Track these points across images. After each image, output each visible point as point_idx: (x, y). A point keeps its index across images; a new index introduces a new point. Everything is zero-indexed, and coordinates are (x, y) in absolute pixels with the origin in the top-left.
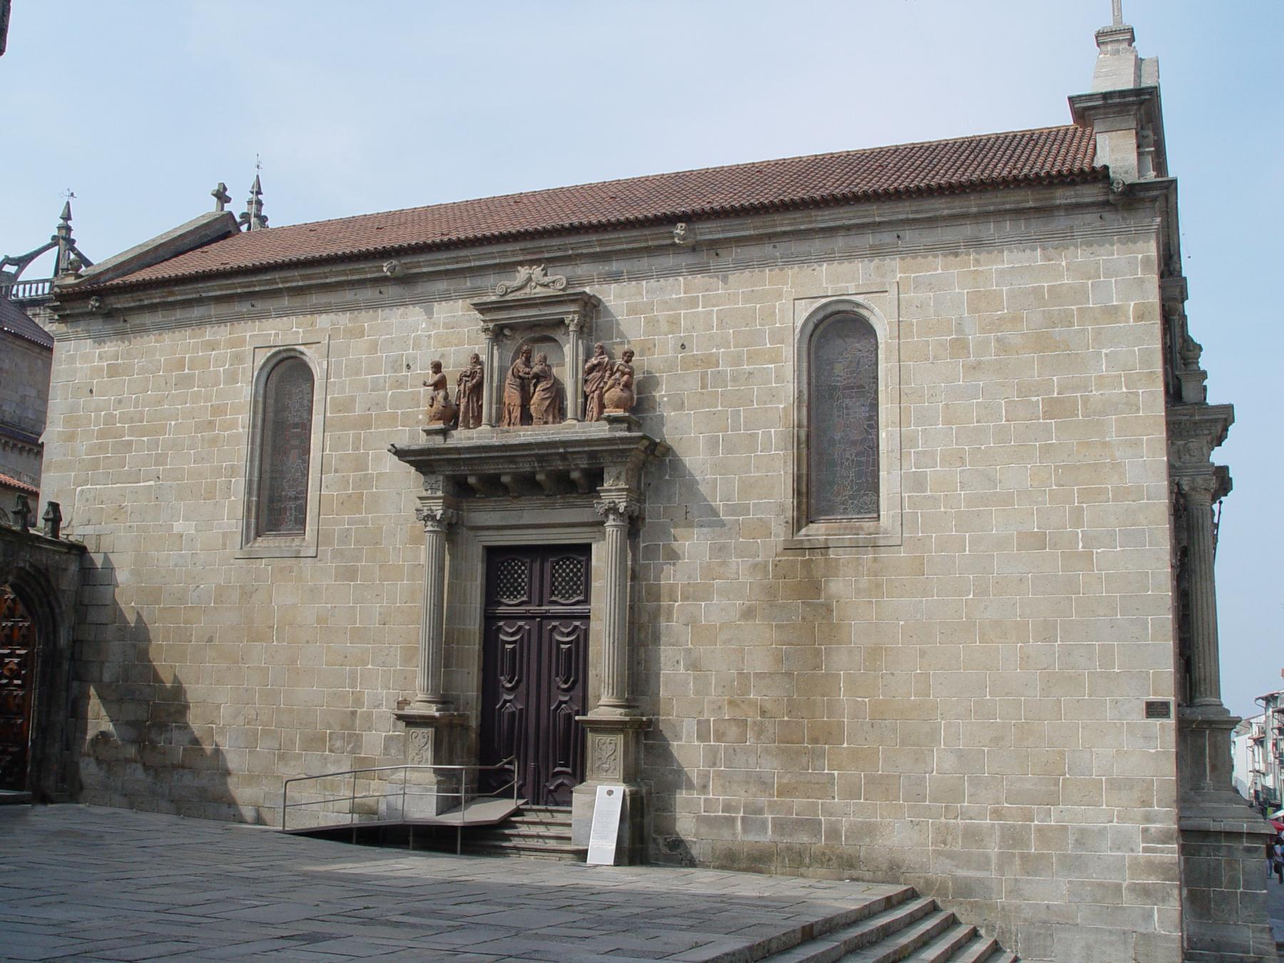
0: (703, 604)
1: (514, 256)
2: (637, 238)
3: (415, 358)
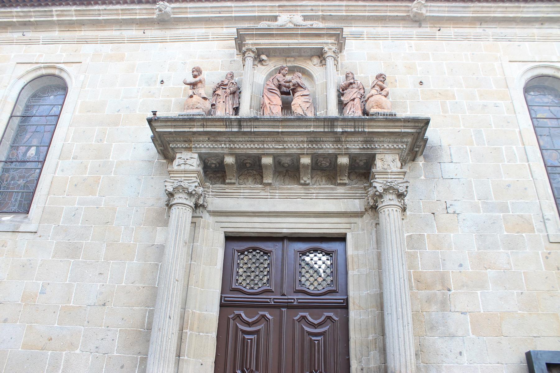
0: (479, 292)
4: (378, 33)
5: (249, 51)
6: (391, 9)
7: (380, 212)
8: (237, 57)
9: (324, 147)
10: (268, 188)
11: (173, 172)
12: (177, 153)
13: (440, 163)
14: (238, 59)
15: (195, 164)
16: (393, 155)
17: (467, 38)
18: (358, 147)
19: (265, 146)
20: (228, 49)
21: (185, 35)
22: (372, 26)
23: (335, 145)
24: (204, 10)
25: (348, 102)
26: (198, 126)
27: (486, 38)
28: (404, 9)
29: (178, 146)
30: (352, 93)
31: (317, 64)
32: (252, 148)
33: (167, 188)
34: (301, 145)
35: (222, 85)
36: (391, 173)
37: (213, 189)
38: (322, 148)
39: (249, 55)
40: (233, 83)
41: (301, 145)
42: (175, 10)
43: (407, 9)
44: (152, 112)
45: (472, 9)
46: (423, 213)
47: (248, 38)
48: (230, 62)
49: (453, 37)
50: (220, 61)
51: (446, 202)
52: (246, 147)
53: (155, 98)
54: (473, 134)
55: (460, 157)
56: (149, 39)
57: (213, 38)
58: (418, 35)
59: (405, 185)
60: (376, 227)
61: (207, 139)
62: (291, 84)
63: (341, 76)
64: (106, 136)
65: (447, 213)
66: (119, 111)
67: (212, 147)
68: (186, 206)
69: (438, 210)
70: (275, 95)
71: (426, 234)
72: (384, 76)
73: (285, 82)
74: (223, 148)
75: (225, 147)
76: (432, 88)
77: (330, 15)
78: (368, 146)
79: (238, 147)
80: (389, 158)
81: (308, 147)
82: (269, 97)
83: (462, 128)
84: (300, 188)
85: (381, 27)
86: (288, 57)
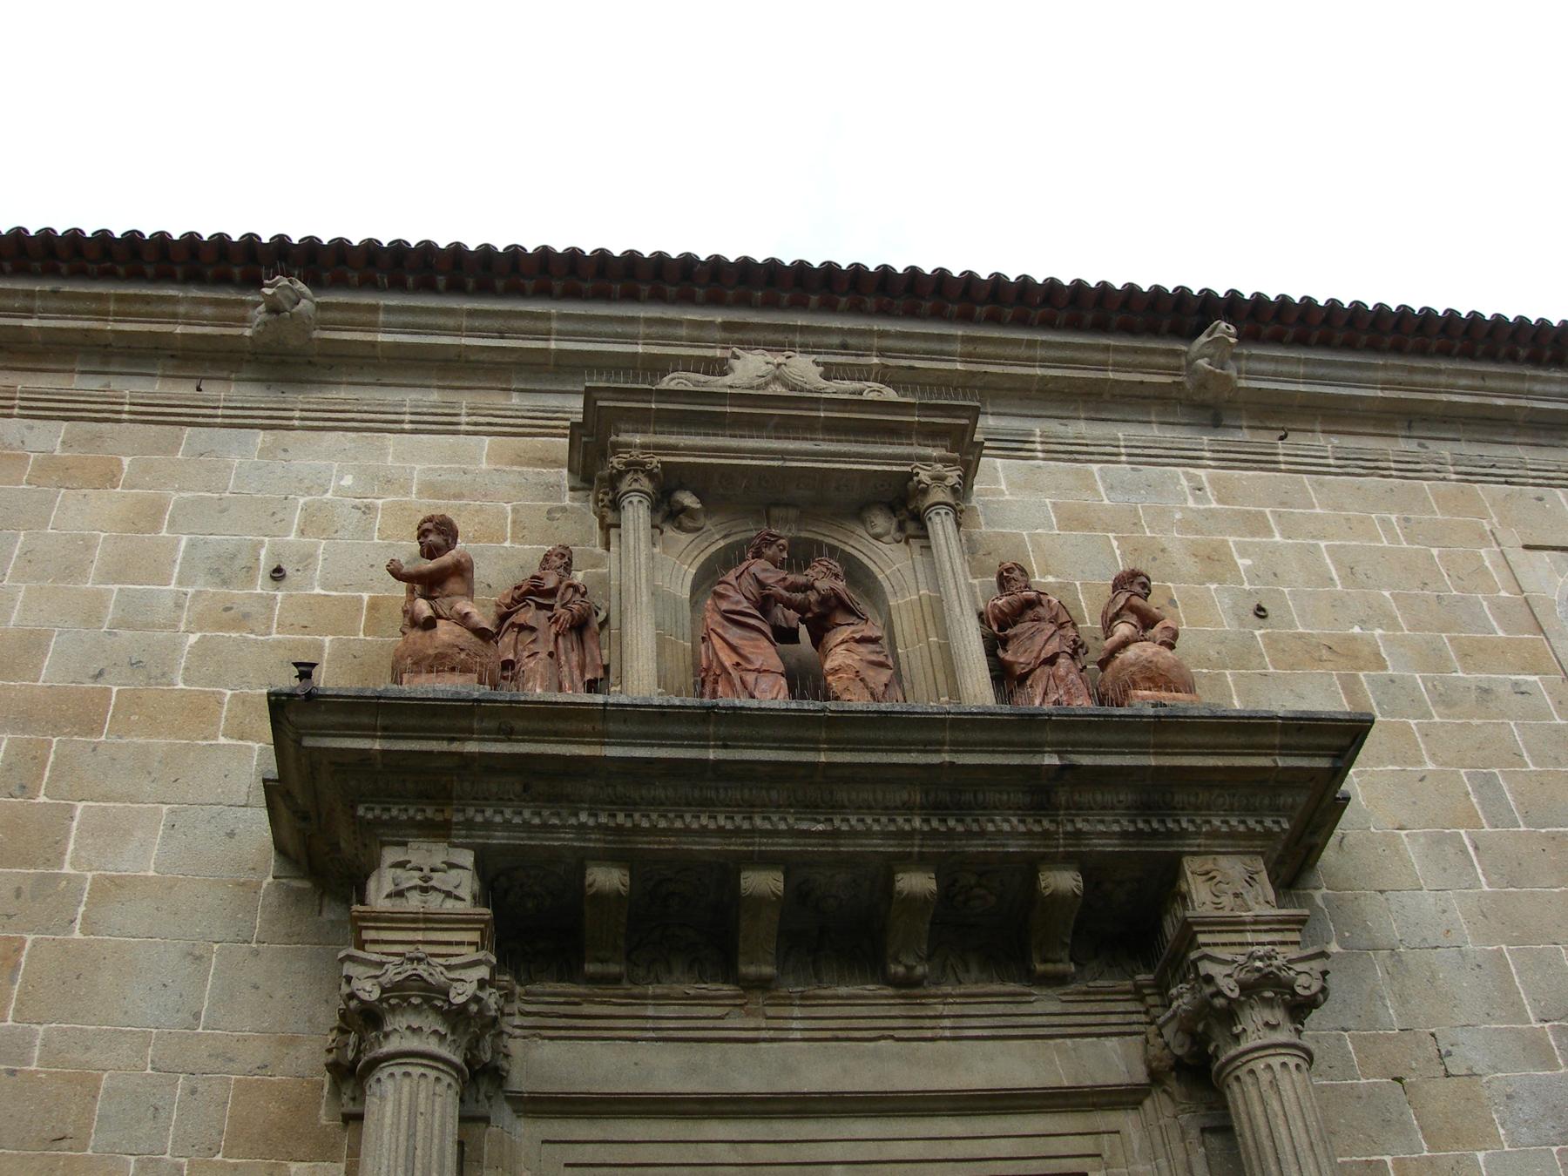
1: (694, 342)
2: (1078, 355)
3: (307, 559)
4: (1083, 438)
5: (636, 471)
6: (1120, 358)
7: (1231, 1079)
8: (573, 499)
9: (990, 827)
10: (758, 999)
11: (376, 919)
12: (384, 844)
13: (1381, 892)
14: (577, 504)
15: (465, 892)
16: (1246, 859)
17: (1377, 468)
18: (1116, 828)
19: (758, 822)
20: (536, 466)
21: (365, 408)
22: (1055, 413)
23: (1029, 820)
24: (441, 321)
25: (1032, 671)
26: (485, 735)
27: (1437, 472)
28: (1162, 360)
29: (395, 812)
30: (1040, 640)
31: (888, 533)
32: (703, 831)
33: (356, 984)
34: (900, 820)
35: (533, 593)
36: (1255, 923)
37: (527, 1002)
38: (982, 834)
39: (636, 486)
40: (576, 588)
41: (900, 820)
42: (330, 315)
43: (1173, 361)
44: (297, 665)
45: (1381, 375)
46: (1363, 1081)
47: (628, 427)
48: (549, 512)
49: (1331, 461)
50: (509, 507)
51: (1433, 1035)
52: (678, 824)
53: (252, 632)
54: (1470, 789)
55: (1445, 870)
56: (220, 412)
57: (476, 424)
58: (1218, 451)
59: (1317, 965)
60: (1203, 1144)
61: (518, 788)
62: (813, 597)
63: (975, 582)
64: (47, 774)
65: (1448, 1075)
66: (101, 674)
67: (537, 821)
68: (440, 1066)
69: (1414, 1065)
70: (755, 635)
71: (1388, 1159)
72: (1144, 580)
73: (787, 589)
74: (583, 826)
75: (591, 822)
76: (1301, 630)
77: (912, 368)
78: (1155, 825)
79: (645, 824)
80: (1232, 867)
81: (926, 828)
82: (734, 641)
83: (1431, 766)
84: (886, 997)
85: (1086, 419)
86: (777, 504)
